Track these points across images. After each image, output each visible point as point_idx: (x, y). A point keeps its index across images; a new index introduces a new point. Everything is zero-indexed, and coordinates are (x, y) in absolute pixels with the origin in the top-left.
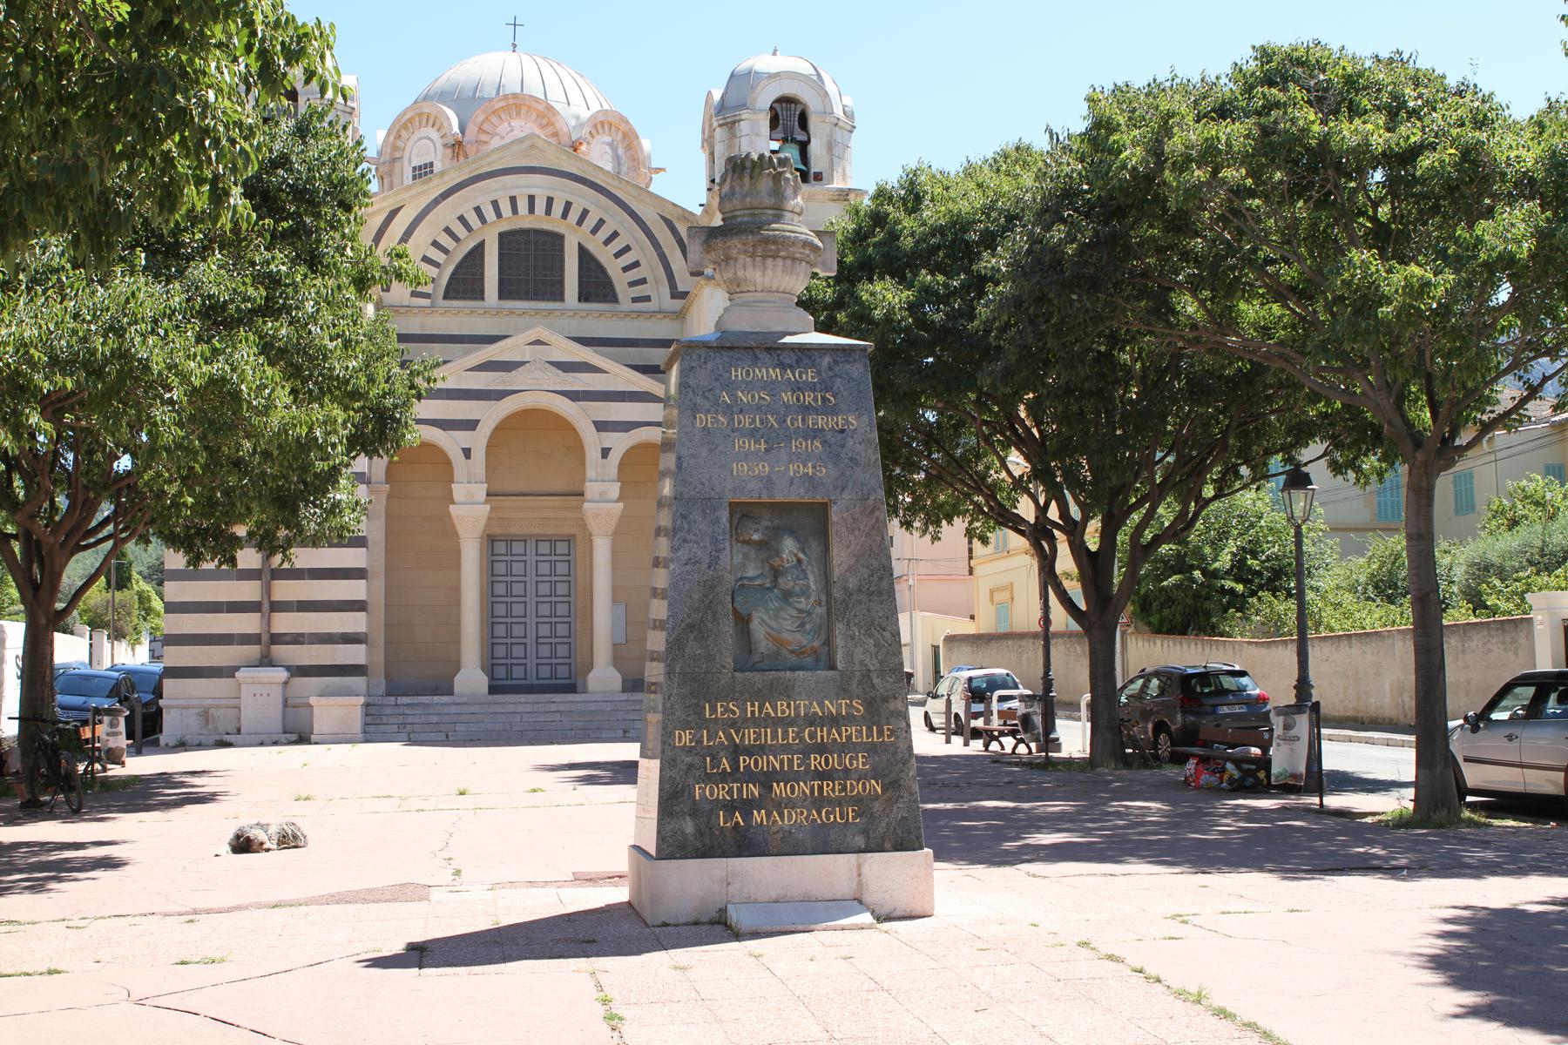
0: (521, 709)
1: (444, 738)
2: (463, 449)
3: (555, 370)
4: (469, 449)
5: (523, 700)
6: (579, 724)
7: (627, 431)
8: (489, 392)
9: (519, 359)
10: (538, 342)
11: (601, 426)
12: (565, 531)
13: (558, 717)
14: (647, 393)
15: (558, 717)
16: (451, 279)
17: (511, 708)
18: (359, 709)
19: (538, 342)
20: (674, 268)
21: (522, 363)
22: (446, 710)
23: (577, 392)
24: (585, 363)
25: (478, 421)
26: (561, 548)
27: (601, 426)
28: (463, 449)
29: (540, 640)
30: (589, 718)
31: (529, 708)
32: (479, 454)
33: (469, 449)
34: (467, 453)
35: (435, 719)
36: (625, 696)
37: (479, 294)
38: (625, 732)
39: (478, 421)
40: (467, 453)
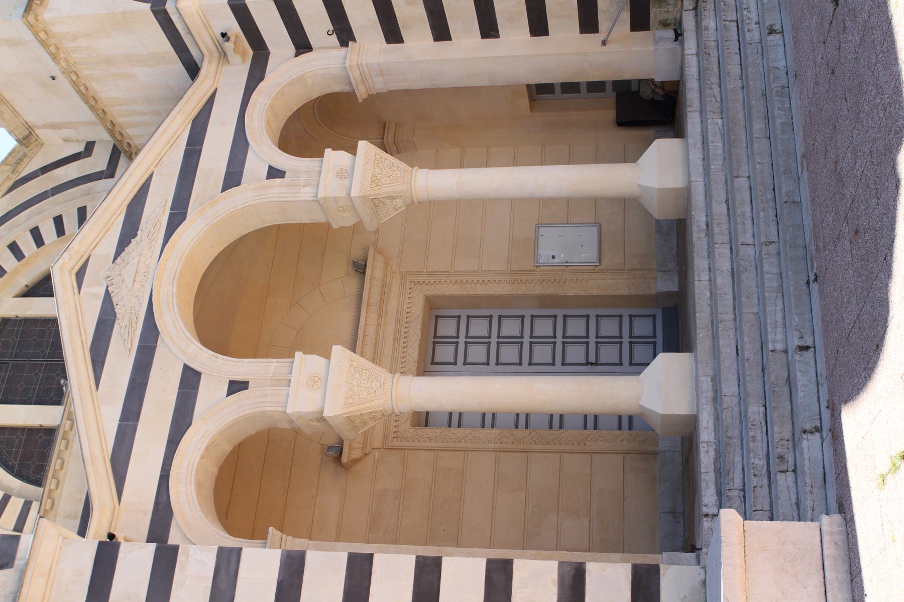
0: (724, 264)
1: (809, 355)
2: (230, 392)
3: (128, 249)
4: (232, 383)
5: (705, 277)
6: (758, 126)
7: (246, 144)
8: (140, 349)
9: (99, 303)
10: (80, 275)
11: (233, 178)
12: (418, 308)
13: (742, 183)
14: (194, 121)
15: (742, 183)
16: (19, 476)
17: (724, 282)
18: (752, 524)
19: (80, 275)
20: (75, 176)
21: (108, 296)
22: (730, 417)
23: (171, 216)
24: (130, 206)
25: (186, 368)
26: (447, 328)
27: (233, 178)
28: (230, 392)
29: (592, 359)
30: (741, 133)
31: (722, 252)
32: (241, 368)
33: (232, 383)
34: (237, 387)
35: (755, 410)
36: (692, 121)
37: (48, 435)
38: (772, 31)
39: (186, 368)
40: (237, 387)
